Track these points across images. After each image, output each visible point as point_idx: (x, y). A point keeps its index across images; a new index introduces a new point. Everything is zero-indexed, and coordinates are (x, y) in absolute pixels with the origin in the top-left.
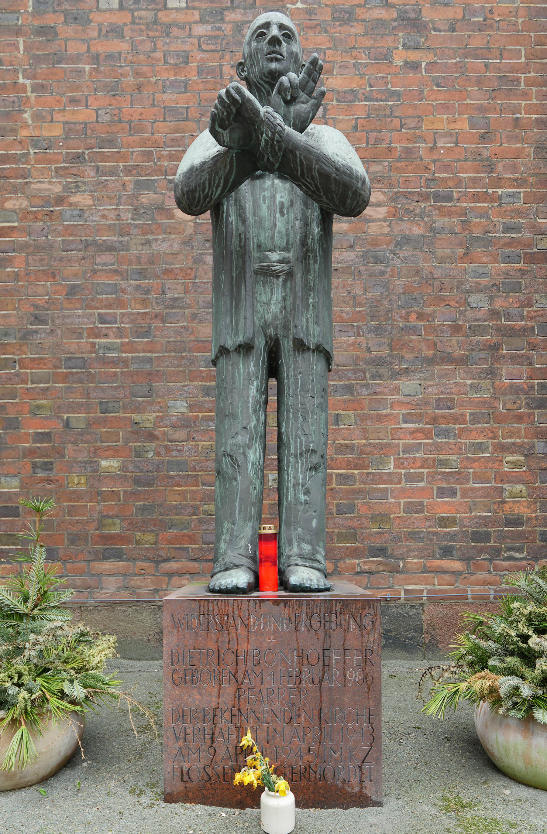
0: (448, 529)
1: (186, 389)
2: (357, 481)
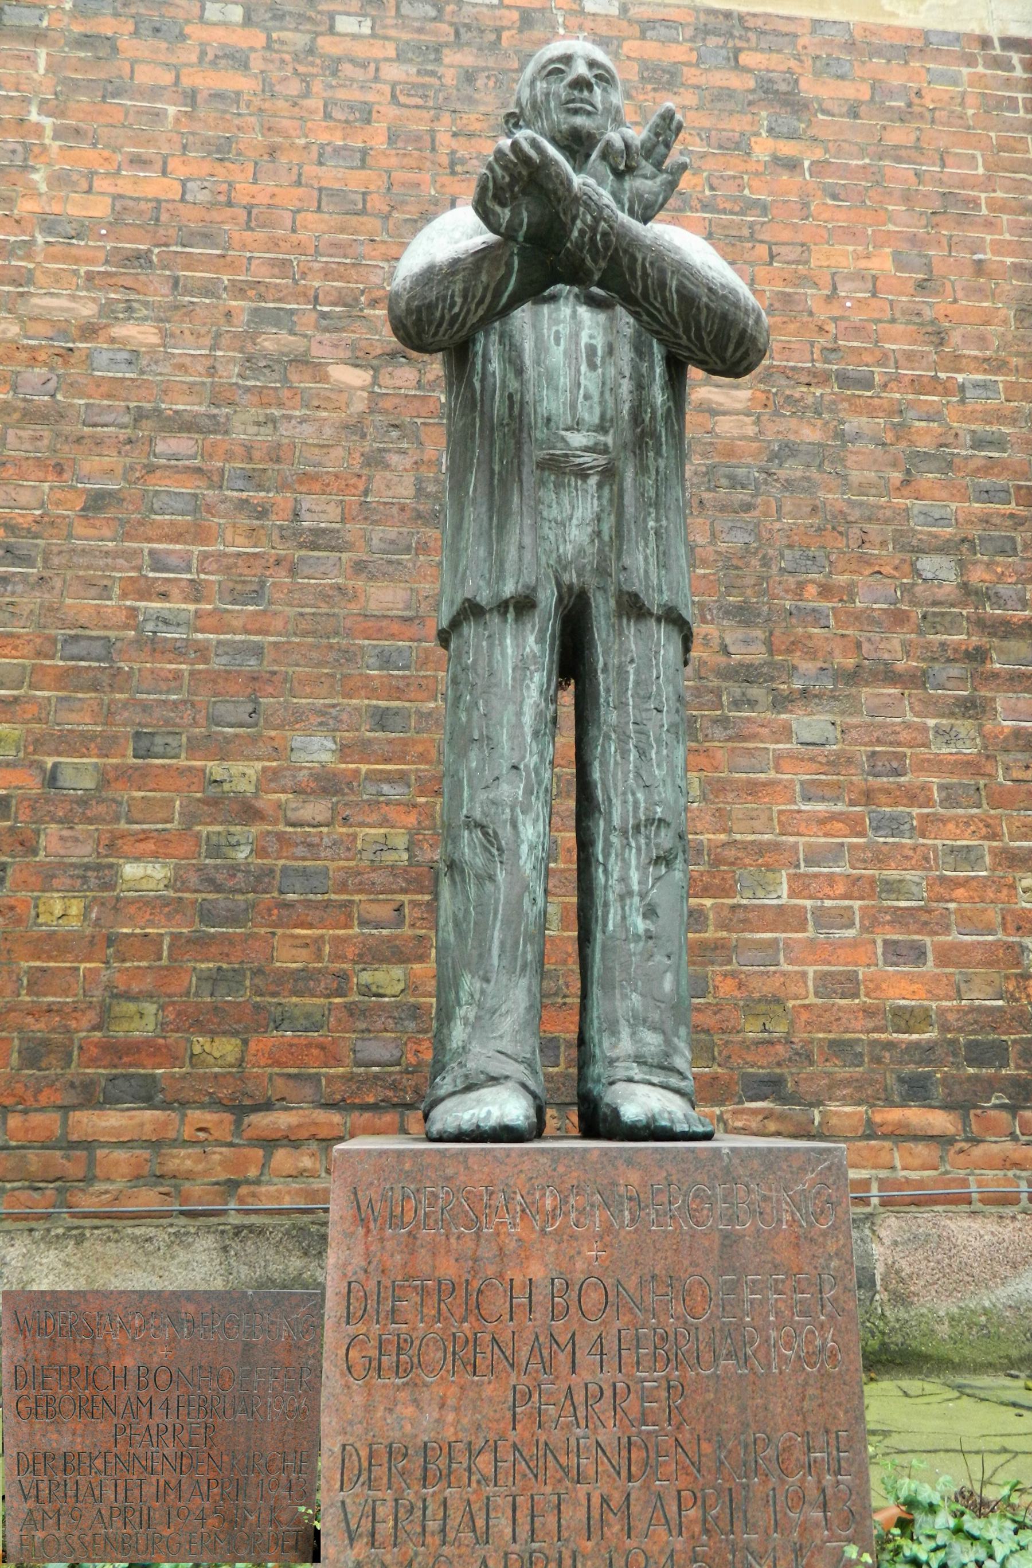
0: (915, 1037)
1: (333, 711)
2: (710, 922)
